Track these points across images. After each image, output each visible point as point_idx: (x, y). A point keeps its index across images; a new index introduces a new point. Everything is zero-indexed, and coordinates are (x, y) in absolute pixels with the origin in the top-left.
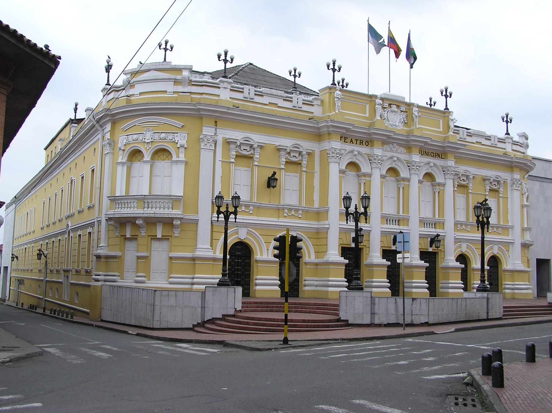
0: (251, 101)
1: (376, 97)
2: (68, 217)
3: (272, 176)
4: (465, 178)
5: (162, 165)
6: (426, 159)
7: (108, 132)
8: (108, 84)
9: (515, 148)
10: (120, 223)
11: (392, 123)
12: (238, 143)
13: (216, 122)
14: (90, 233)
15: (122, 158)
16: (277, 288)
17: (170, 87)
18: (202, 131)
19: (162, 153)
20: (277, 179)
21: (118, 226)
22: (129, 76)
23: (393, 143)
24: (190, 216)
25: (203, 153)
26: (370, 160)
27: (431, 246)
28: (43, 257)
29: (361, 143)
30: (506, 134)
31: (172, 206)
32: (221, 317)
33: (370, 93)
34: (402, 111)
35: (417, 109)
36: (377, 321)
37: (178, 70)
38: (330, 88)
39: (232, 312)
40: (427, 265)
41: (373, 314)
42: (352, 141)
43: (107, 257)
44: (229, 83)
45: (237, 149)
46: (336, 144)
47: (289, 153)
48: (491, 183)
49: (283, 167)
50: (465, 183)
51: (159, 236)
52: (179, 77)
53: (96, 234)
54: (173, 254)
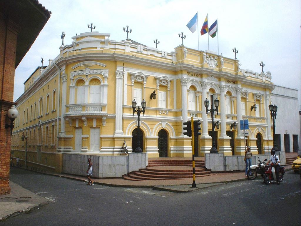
0: (141, 53)
1: (203, 52)
2: (39, 118)
3: (153, 93)
4: (245, 94)
5: (94, 88)
6: (228, 84)
7: (63, 70)
8: (63, 44)
9: (267, 79)
10: (73, 119)
11: (211, 66)
12: (136, 76)
13: (123, 64)
14: (53, 126)
15: (73, 84)
16: (157, 152)
17: (100, 46)
18: (116, 69)
19: (95, 81)
20: (156, 95)
21: (70, 121)
22: (75, 40)
24: (111, 114)
25: (117, 81)
26: (201, 84)
27: (231, 129)
28: (25, 139)
29: (197, 75)
30: (262, 72)
31: (102, 109)
32: (138, 170)
33: (200, 50)
34: (215, 60)
35: (223, 58)
36: (227, 170)
37: (103, 36)
38: (181, 47)
39: (144, 167)
40: (231, 138)
41: (225, 166)
42: (192, 74)
43: (65, 138)
44: (130, 43)
45: (135, 78)
46: (185, 76)
47: (161, 81)
48: (256, 96)
50: (245, 96)
51: (94, 126)
52: (103, 40)
53: (58, 126)
54: (102, 136)
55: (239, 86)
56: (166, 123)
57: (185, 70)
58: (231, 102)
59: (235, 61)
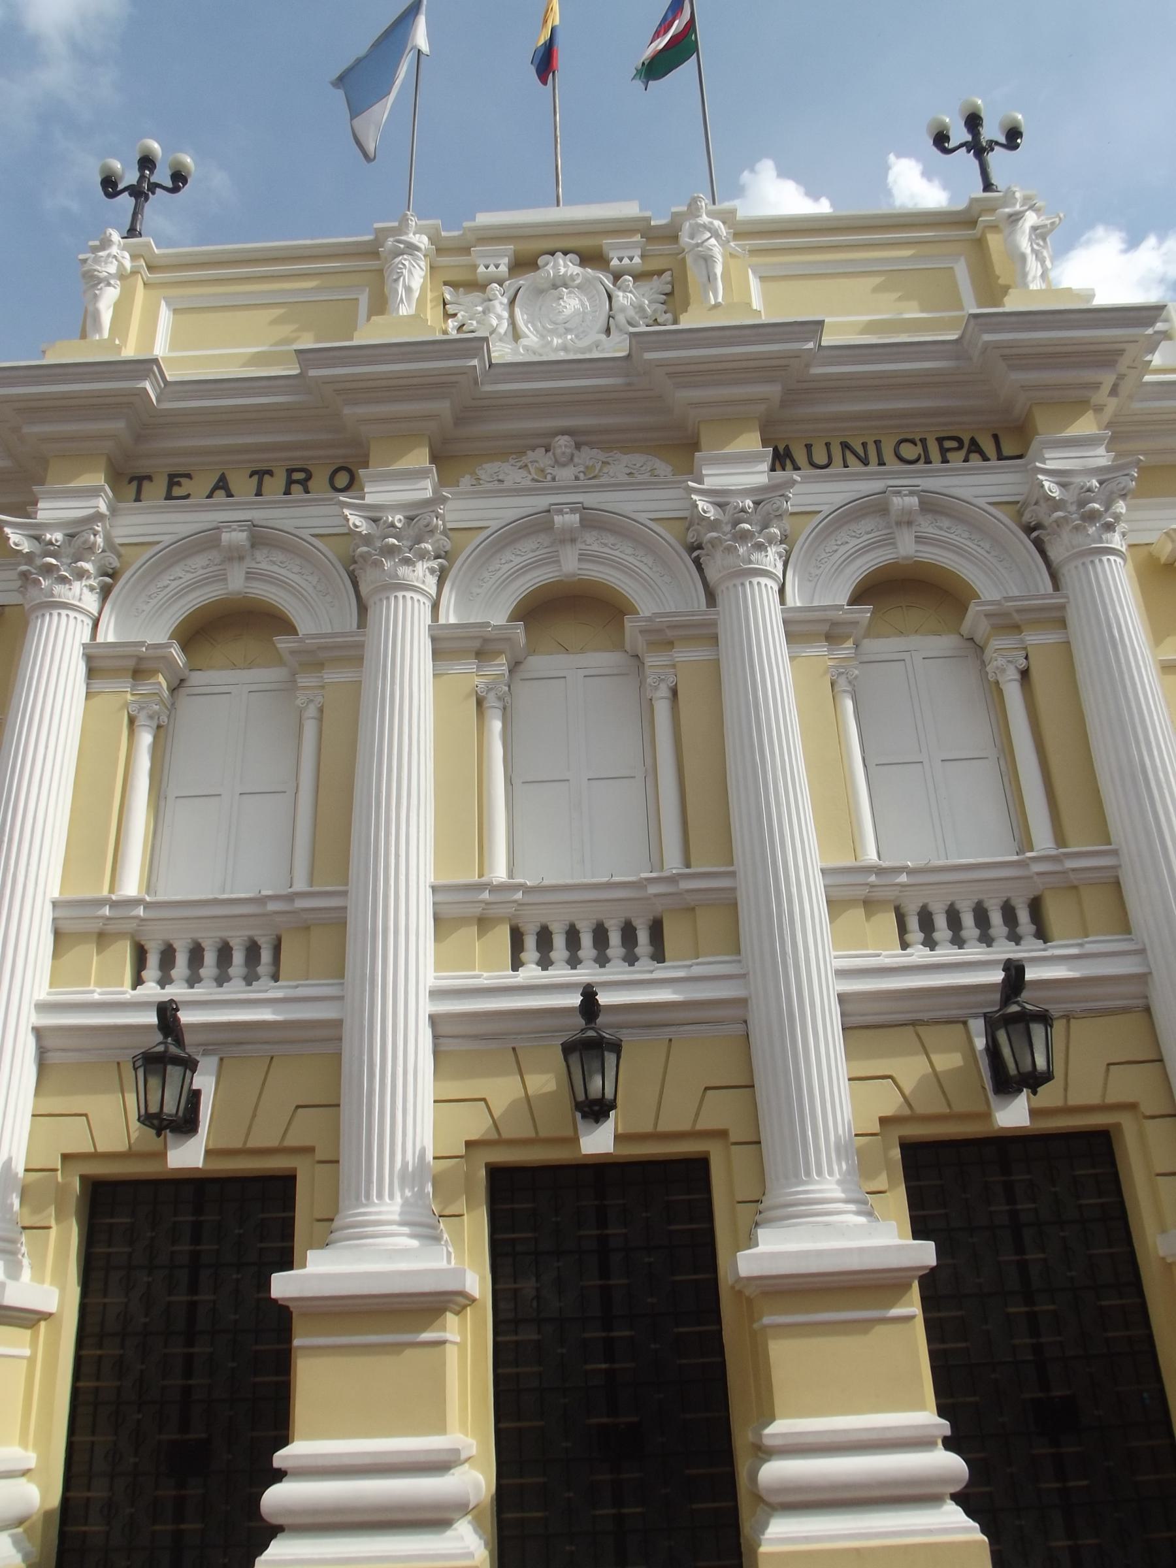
29: (298, 479)
42: (222, 485)
55: (1071, 457)
58: (996, 692)
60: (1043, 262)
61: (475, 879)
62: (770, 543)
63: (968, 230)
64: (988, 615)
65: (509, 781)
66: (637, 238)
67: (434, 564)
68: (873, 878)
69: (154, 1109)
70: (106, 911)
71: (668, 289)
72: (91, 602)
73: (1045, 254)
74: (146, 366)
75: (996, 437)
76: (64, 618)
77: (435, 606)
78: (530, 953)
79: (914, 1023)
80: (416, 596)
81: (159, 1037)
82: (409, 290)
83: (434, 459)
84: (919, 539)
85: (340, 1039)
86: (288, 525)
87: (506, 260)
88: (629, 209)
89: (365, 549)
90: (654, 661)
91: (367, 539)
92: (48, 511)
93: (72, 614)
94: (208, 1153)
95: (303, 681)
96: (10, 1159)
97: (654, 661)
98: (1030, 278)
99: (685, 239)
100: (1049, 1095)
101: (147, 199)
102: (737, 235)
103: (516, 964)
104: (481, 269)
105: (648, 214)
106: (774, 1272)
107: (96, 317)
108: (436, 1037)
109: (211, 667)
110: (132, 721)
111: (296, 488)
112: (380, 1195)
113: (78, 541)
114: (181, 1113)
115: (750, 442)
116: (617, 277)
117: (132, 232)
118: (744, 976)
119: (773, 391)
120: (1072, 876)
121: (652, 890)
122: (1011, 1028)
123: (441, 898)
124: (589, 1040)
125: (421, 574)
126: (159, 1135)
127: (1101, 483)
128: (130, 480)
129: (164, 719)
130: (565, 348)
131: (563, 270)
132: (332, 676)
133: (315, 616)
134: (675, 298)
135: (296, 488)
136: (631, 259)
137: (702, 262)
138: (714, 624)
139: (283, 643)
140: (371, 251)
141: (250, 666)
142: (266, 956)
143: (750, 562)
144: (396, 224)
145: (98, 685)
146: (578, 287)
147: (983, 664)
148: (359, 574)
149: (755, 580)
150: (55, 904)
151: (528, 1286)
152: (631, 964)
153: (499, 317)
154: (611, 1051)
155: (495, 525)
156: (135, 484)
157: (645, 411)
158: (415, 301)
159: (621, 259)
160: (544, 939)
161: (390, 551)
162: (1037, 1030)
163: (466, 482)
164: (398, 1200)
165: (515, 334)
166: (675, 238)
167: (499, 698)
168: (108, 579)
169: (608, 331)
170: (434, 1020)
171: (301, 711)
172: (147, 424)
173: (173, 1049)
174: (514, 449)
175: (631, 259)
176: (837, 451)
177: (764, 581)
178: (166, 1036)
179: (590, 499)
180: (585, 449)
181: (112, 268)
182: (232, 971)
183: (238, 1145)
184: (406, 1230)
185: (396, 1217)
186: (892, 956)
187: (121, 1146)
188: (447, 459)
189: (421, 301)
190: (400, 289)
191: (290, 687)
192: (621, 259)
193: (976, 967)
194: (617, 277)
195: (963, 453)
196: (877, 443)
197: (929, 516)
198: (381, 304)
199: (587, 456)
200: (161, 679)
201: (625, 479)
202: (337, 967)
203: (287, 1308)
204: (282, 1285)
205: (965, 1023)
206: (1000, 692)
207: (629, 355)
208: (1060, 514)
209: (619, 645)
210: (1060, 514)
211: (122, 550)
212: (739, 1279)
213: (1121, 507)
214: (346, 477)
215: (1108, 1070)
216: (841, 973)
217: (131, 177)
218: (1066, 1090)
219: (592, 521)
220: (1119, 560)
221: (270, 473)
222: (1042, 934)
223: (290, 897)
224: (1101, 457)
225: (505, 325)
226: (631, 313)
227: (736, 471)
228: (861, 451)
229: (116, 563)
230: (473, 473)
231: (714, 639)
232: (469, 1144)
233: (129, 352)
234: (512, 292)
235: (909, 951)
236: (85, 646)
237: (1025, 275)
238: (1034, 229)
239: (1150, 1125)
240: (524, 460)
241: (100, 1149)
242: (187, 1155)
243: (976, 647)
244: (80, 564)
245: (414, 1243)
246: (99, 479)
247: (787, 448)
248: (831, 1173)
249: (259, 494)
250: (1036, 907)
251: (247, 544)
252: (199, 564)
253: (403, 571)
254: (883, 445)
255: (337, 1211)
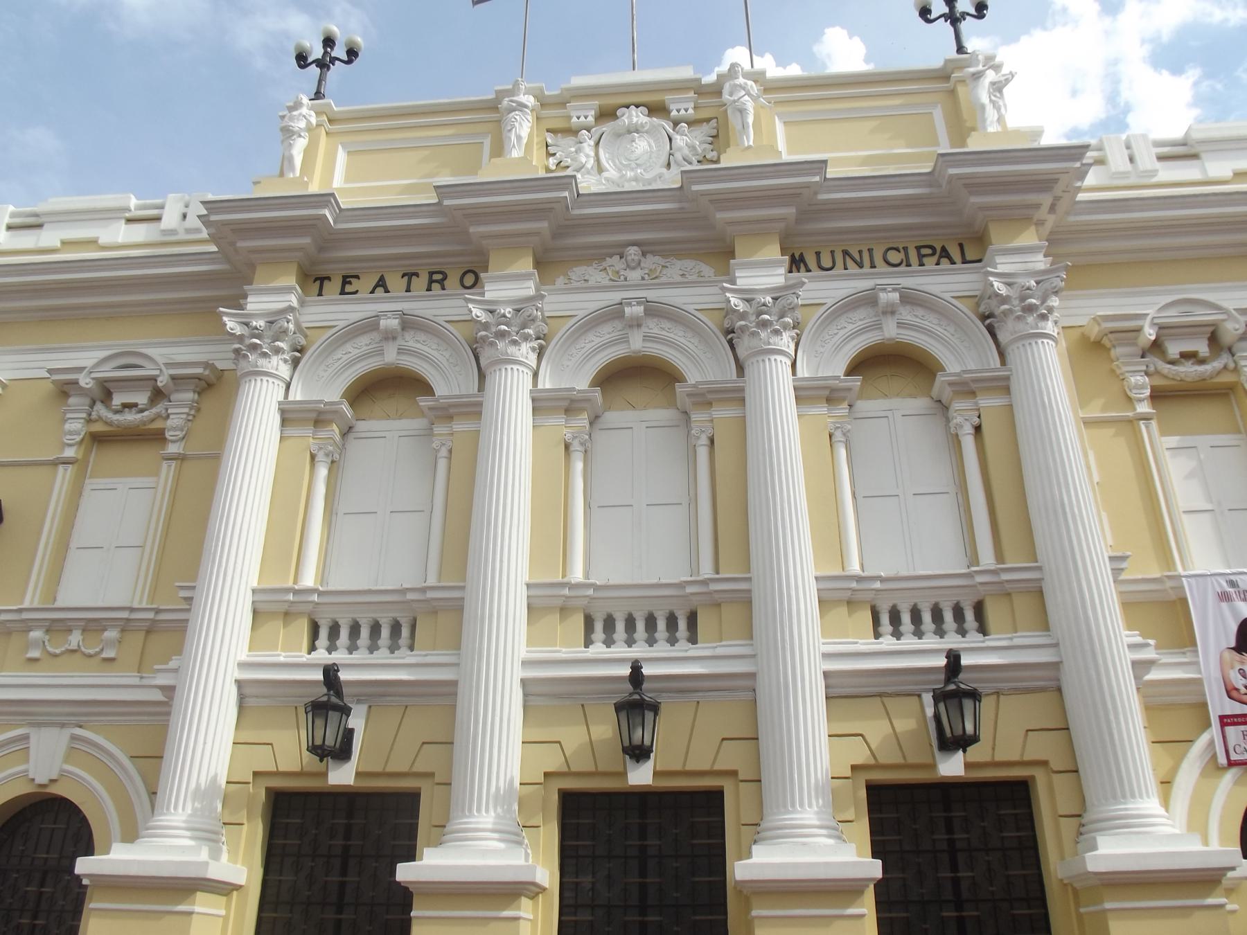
23: (619, 250)
29: (437, 279)
42: (381, 283)
49: (70, 453)
55: (1017, 260)
56: (74, 738)
57: (275, 259)
59: (943, 75)
60: (999, 109)
61: (560, 579)
62: (785, 329)
63: (948, 83)
64: (951, 384)
65: (588, 506)
66: (691, 94)
67: (535, 344)
68: (854, 585)
69: (318, 742)
70: (291, 597)
71: (714, 132)
72: (284, 370)
73: (1001, 103)
74: (326, 199)
75: (961, 246)
76: (265, 383)
77: (536, 375)
78: (599, 634)
79: (880, 695)
80: (521, 368)
81: (325, 690)
82: (519, 138)
83: (538, 264)
84: (900, 325)
85: (456, 694)
86: (428, 313)
87: (593, 113)
88: (686, 73)
89: (483, 333)
90: (698, 417)
91: (486, 326)
92: (256, 303)
93: (271, 380)
94: (358, 774)
95: (439, 429)
96: (216, 775)
97: (698, 417)
98: (988, 122)
99: (726, 96)
100: (976, 753)
101: (329, 68)
102: (767, 90)
103: (588, 643)
104: (574, 119)
105: (698, 76)
106: (761, 878)
107: (291, 159)
108: (525, 695)
109: (370, 418)
110: (313, 457)
111: (435, 286)
112: (479, 810)
113: (276, 327)
114: (338, 745)
115: (773, 251)
116: (676, 124)
117: (318, 95)
118: (754, 656)
119: (790, 211)
120: (981, 588)
121: (689, 590)
122: (948, 702)
123: (534, 592)
124: (636, 702)
125: (525, 352)
126: (321, 761)
127: (1038, 283)
128: (314, 280)
129: (336, 456)
130: (636, 179)
131: (635, 120)
132: (459, 426)
133: (449, 382)
134: (720, 139)
135: (435, 285)
136: (686, 110)
137: (738, 114)
138: (742, 390)
139: (424, 402)
140: (492, 106)
141: (400, 418)
142: (405, 632)
143: (769, 344)
144: (510, 87)
145: (290, 431)
146: (647, 132)
147: (948, 420)
148: (479, 351)
149: (773, 358)
150: (254, 591)
151: (586, 880)
152: (673, 645)
153: (587, 156)
154: (650, 710)
155: (581, 314)
156: (318, 282)
157: (694, 226)
158: (524, 150)
159: (678, 111)
160: (609, 624)
161: (502, 335)
162: (968, 704)
163: (560, 282)
164: (492, 813)
165: (600, 169)
166: (719, 93)
167: (582, 444)
168: (298, 354)
169: (669, 165)
170: (524, 682)
171: (437, 451)
172: (327, 239)
173: (334, 700)
174: (597, 255)
175: (686, 110)
176: (839, 258)
177: (779, 358)
178: (329, 690)
179: (651, 295)
180: (649, 256)
181: (302, 124)
182: (380, 642)
183: (379, 769)
184: (496, 835)
185: (490, 826)
186: (867, 643)
187: (297, 768)
188: (545, 264)
189: (529, 146)
190: (513, 137)
191: (429, 434)
192: (678, 111)
193: (925, 652)
194: (676, 124)
195: (935, 258)
196: (870, 251)
197: (908, 307)
198: (499, 149)
199: (651, 261)
200: (335, 427)
201: (680, 279)
202: (455, 641)
203: (407, 888)
204: (405, 872)
205: (919, 696)
206: (959, 442)
207: (682, 187)
208: (1006, 307)
209: (672, 403)
210: (1006, 307)
211: (308, 332)
212: (736, 882)
213: (1054, 302)
214: (472, 278)
215: (1026, 735)
216: (827, 656)
217: (317, 52)
218: (993, 749)
219: (654, 311)
220: (1051, 342)
221: (417, 275)
222: (983, 630)
223: (423, 590)
224: (1040, 262)
225: (591, 162)
226: (686, 151)
227: (761, 273)
228: (857, 257)
229: (303, 342)
230: (566, 275)
231: (743, 400)
232: (546, 775)
233: (314, 188)
234: (596, 137)
235: (881, 640)
236: (280, 403)
237: (984, 120)
238: (993, 84)
239: (1055, 776)
240: (604, 264)
241: (281, 769)
242: (342, 776)
243: (942, 407)
244: (278, 343)
245: (502, 845)
246: (291, 280)
247: (801, 255)
248: (810, 806)
249: (408, 290)
250: (979, 609)
251: (399, 328)
252: (364, 343)
253: (512, 350)
254: (875, 253)
255: (448, 820)
